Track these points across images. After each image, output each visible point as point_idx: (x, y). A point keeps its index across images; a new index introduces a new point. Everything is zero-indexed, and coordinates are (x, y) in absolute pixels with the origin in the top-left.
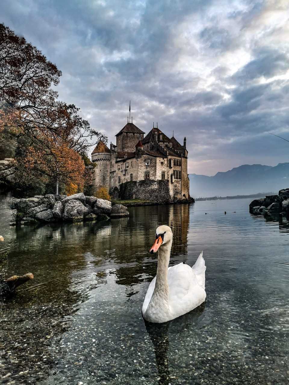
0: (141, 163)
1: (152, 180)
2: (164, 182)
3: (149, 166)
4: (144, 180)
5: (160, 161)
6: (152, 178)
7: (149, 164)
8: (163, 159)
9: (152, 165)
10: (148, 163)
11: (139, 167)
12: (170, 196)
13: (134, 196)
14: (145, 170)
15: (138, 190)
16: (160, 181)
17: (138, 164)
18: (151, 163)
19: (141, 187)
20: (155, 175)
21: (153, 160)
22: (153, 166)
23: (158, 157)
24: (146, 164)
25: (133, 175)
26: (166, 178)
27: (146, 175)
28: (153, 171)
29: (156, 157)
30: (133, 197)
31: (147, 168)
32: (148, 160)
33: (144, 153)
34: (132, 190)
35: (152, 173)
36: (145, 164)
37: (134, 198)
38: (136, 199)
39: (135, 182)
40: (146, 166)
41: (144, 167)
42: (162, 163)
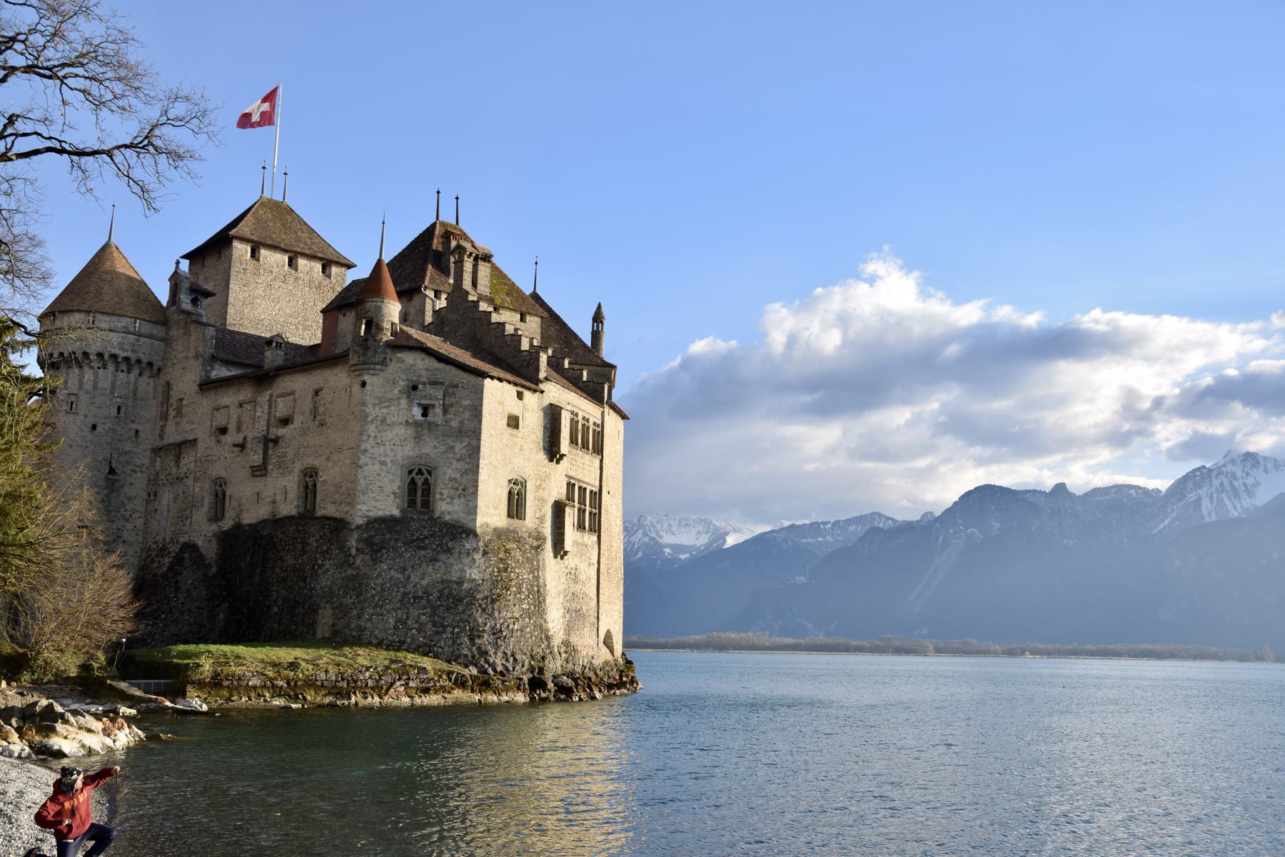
0: (381, 402)
1: (446, 524)
2: (518, 540)
3: (432, 426)
4: (396, 512)
5: (501, 403)
6: (446, 508)
7: (437, 415)
8: (520, 396)
9: (454, 424)
10: (426, 411)
11: (372, 429)
12: (548, 638)
13: (325, 618)
14: (408, 451)
15: (352, 578)
16: (499, 534)
17: (364, 404)
18: (445, 411)
19: (376, 561)
20: (468, 489)
21: (459, 392)
22: (460, 433)
23: (492, 378)
24: (417, 412)
25: (329, 476)
26: (530, 521)
27: (413, 481)
28: (460, 465)
29: (483, 375)
30: (313, 625)
31: (418, 438)
32: (430, 390)
33: (412, 343)
34: (315, 574)
35: (450, 473)
36: (410, 409)
37: (323, 630)
38: (337, 640)
39: (338, 526)
40: (416, 424)
41: (401, 431)
42: (514, 422)
